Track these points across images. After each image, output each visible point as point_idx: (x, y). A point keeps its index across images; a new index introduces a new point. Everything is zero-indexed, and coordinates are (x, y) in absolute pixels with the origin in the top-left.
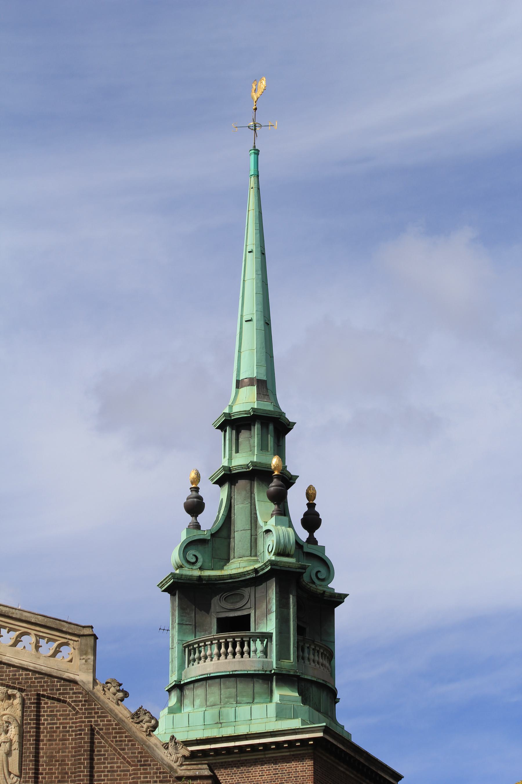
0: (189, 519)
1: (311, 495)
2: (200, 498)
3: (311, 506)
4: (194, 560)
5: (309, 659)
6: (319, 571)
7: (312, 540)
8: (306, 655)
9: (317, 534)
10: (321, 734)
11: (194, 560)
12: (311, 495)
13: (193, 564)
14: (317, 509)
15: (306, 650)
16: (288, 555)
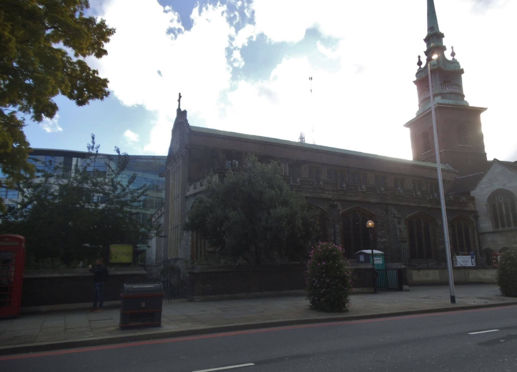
0: (419, 67)
1: (452, 48)
2: (421, 62)
3: (453, 50)
4: (419, 76)
5: (454, 88)
6: (455, 66)
7: (453, 59)
8: (451, 87)
9: (455, 57)
10: (437, 105)
11: (419, 76)
12: (452, 48)
13: (420, 77)
14: (454, 51)
15: (451, 86)
16: (435, 65)
